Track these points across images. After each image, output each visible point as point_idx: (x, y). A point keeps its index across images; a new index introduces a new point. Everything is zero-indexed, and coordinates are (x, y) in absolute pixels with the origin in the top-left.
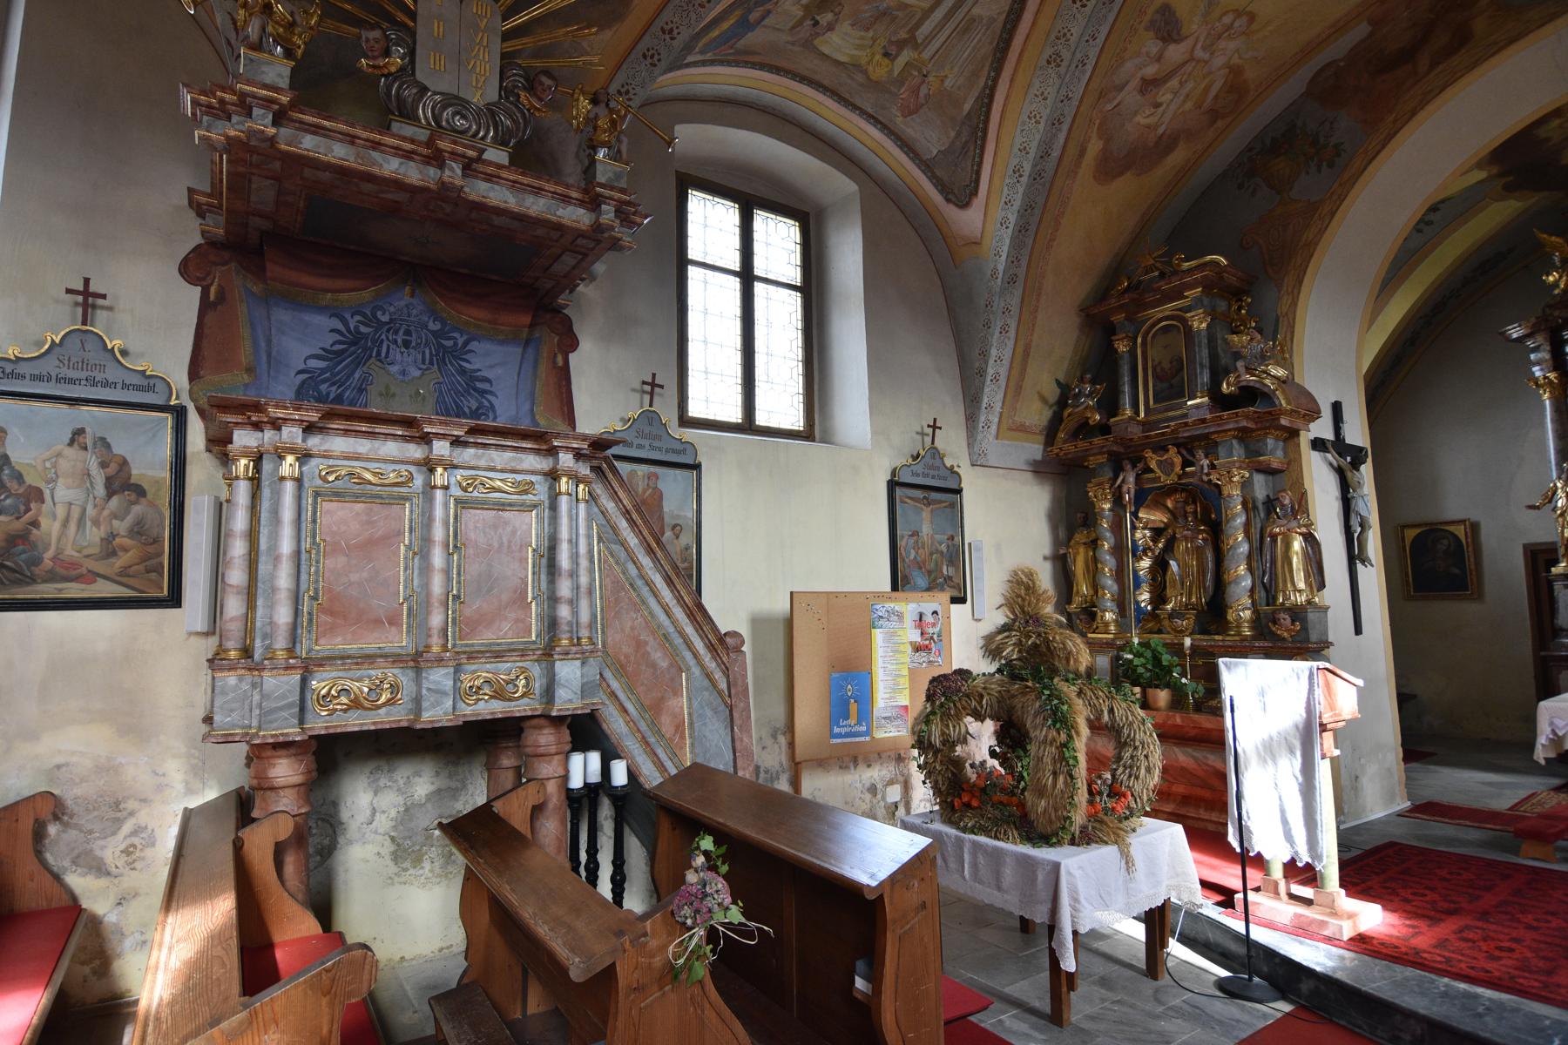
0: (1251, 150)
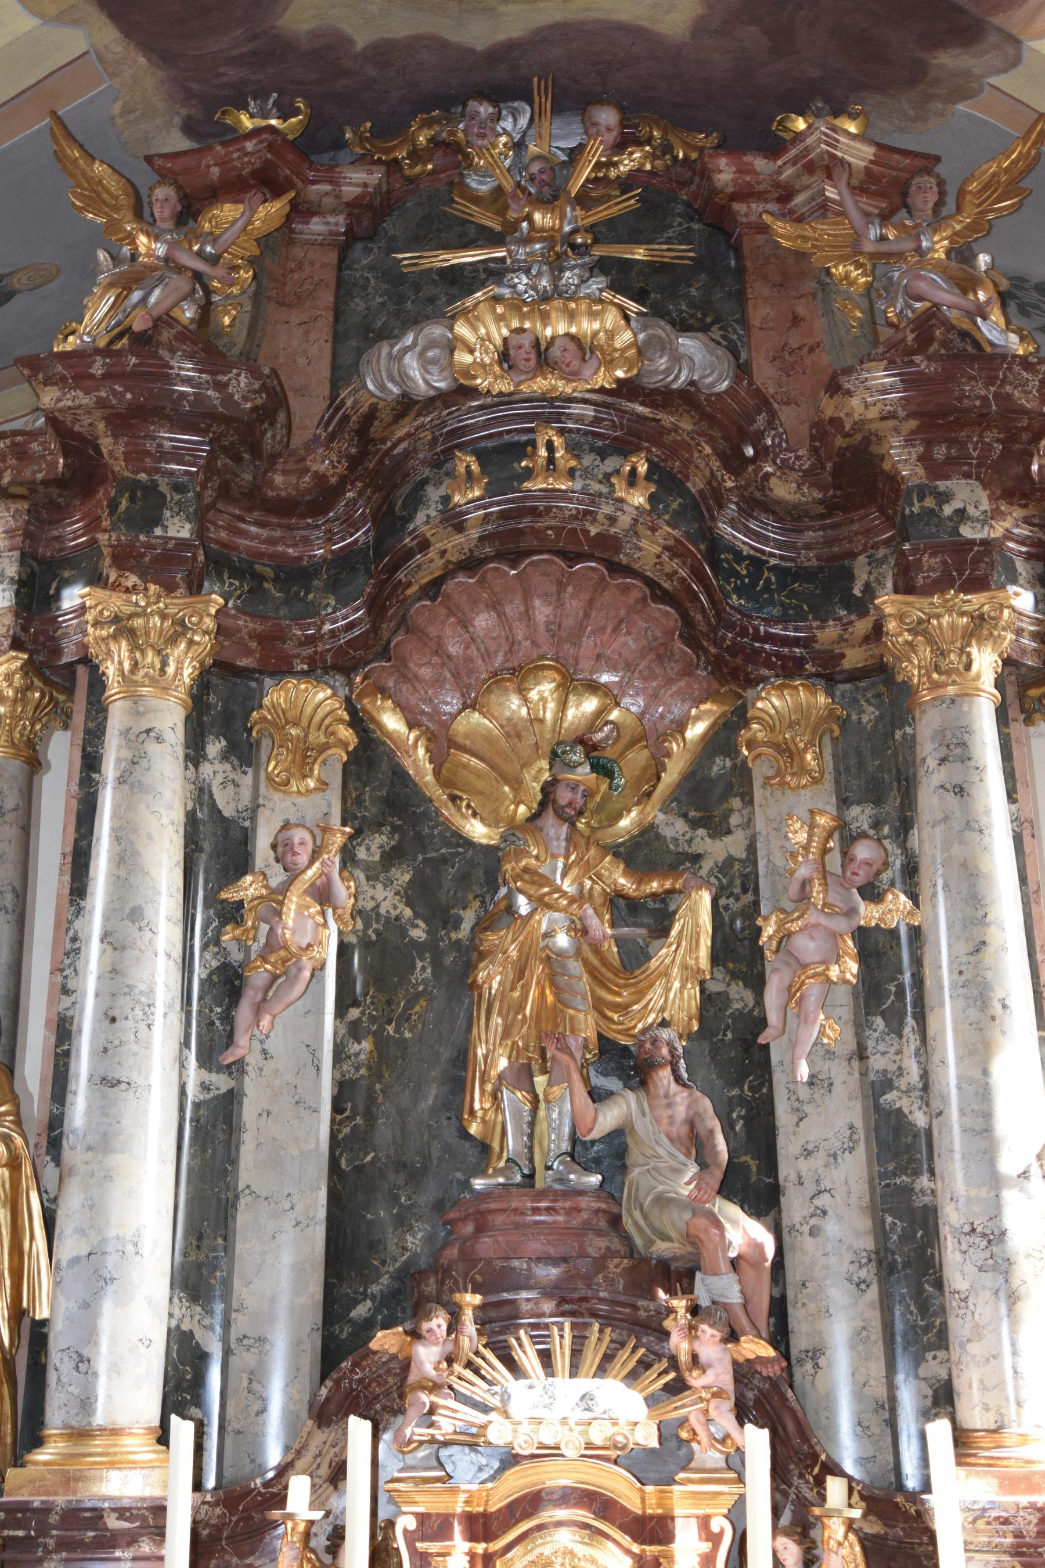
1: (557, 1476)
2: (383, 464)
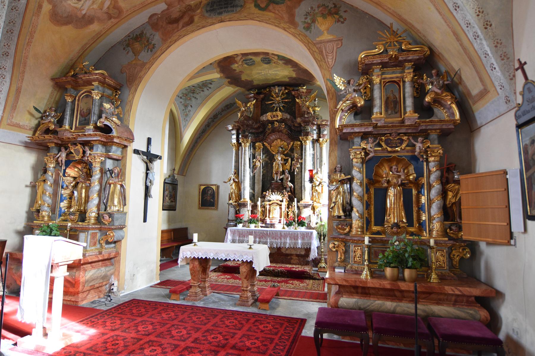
0: (129, 36)
1: (274, 202)
2: (264, 125)
